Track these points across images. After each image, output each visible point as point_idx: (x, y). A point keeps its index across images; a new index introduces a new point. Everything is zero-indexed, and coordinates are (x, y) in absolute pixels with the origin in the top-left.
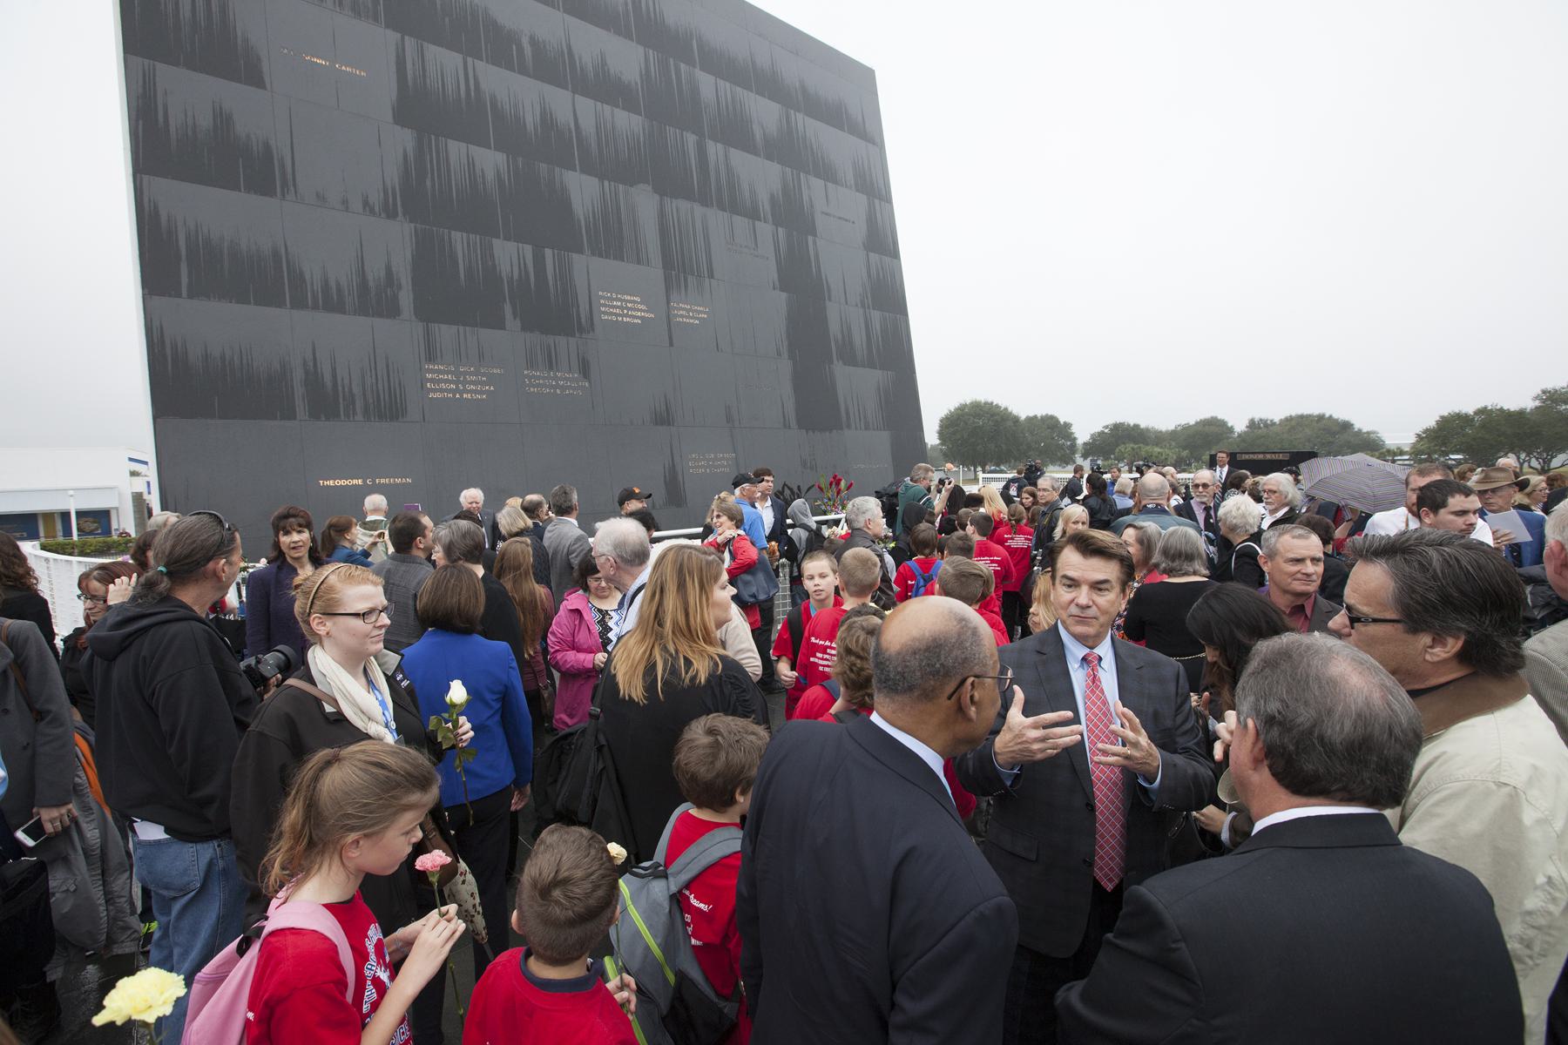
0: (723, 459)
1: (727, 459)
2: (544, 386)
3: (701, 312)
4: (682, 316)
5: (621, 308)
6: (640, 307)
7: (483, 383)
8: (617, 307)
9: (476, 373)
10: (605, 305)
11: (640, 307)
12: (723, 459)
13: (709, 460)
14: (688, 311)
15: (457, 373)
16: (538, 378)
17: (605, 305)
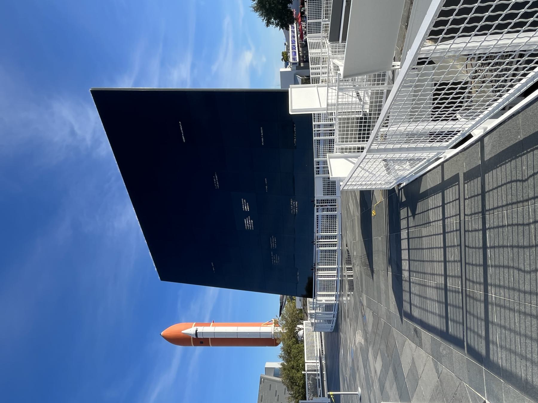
0: (293, 203)
1: (293, 202)
2: (274, 245)
3: (244, 203)
4: (247, 208)
5: (249, 224)
6: (247, 219)
7: (275, 256)
8: (249, 222)
9: (273, 257)
10: (249, 228)
11: (247, 219)
12: (293, 203)
13: (293, 208)
14: (244, 206)
15: (274, 260)
16: (272, 246)
17: (249, 228)
